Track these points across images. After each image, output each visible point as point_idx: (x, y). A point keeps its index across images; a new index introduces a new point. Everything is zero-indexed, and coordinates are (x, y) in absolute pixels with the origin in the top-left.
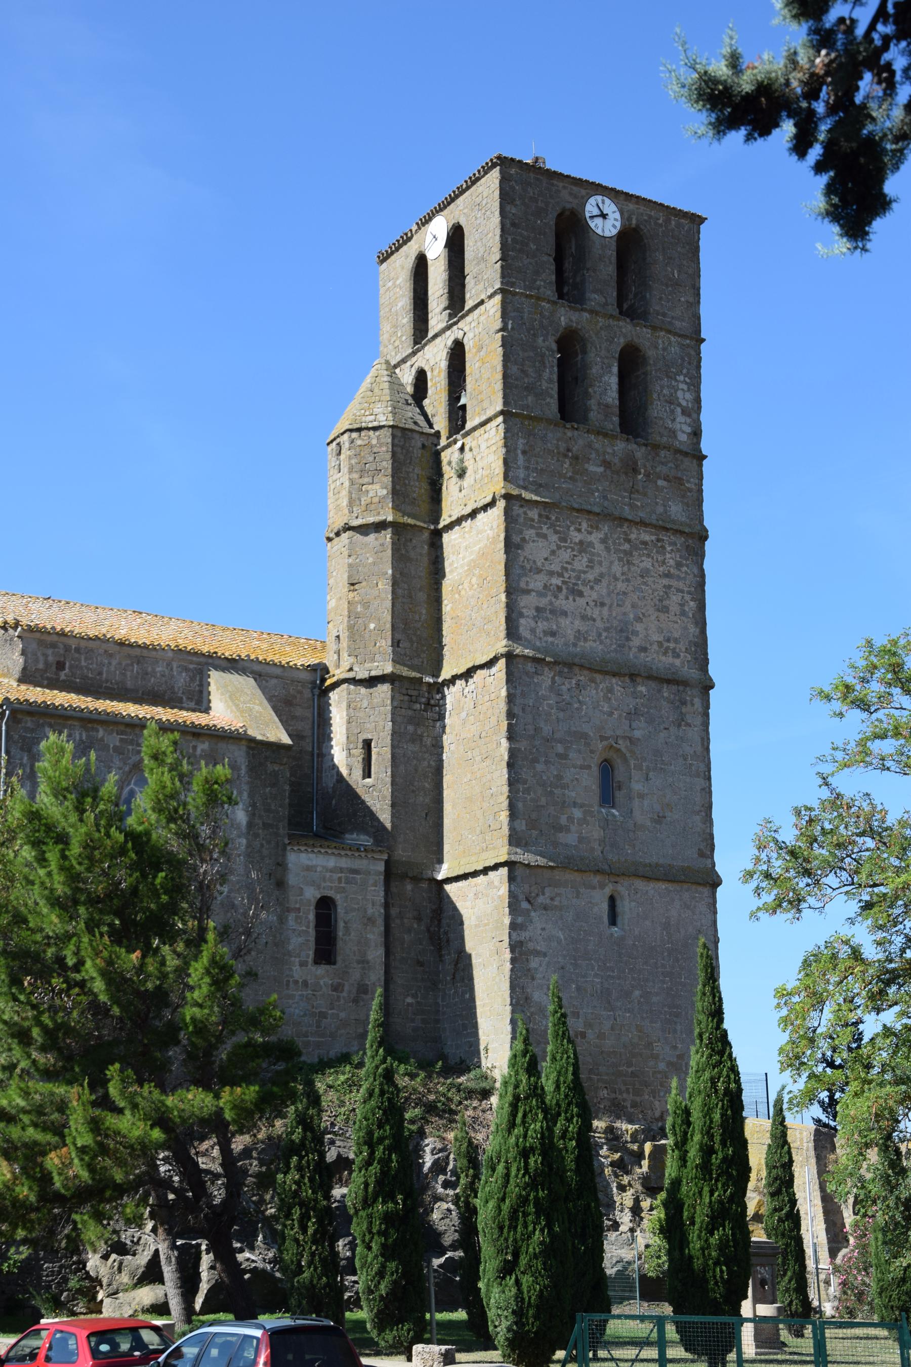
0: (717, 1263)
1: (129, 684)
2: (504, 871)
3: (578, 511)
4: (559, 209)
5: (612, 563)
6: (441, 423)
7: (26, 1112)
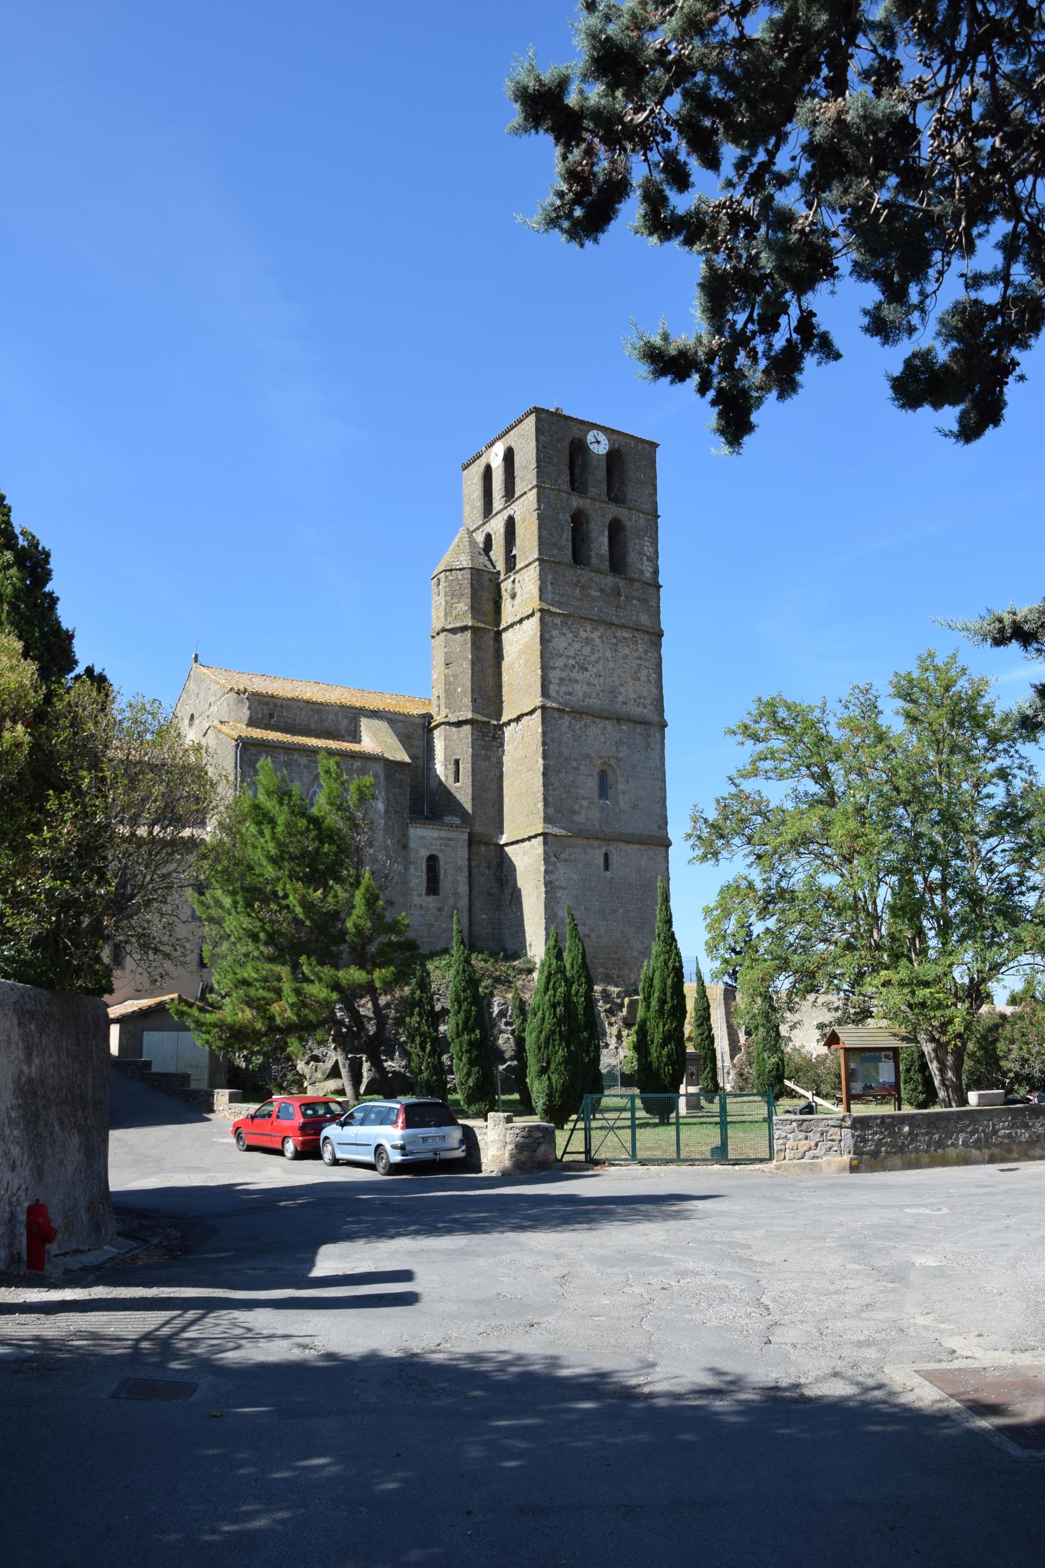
0: (666, 1064)
1: (313, 727)
2: (541, 838)
3: (585, 619)
4: (571, 438)
6: (501, 566)
7: (257, 980)
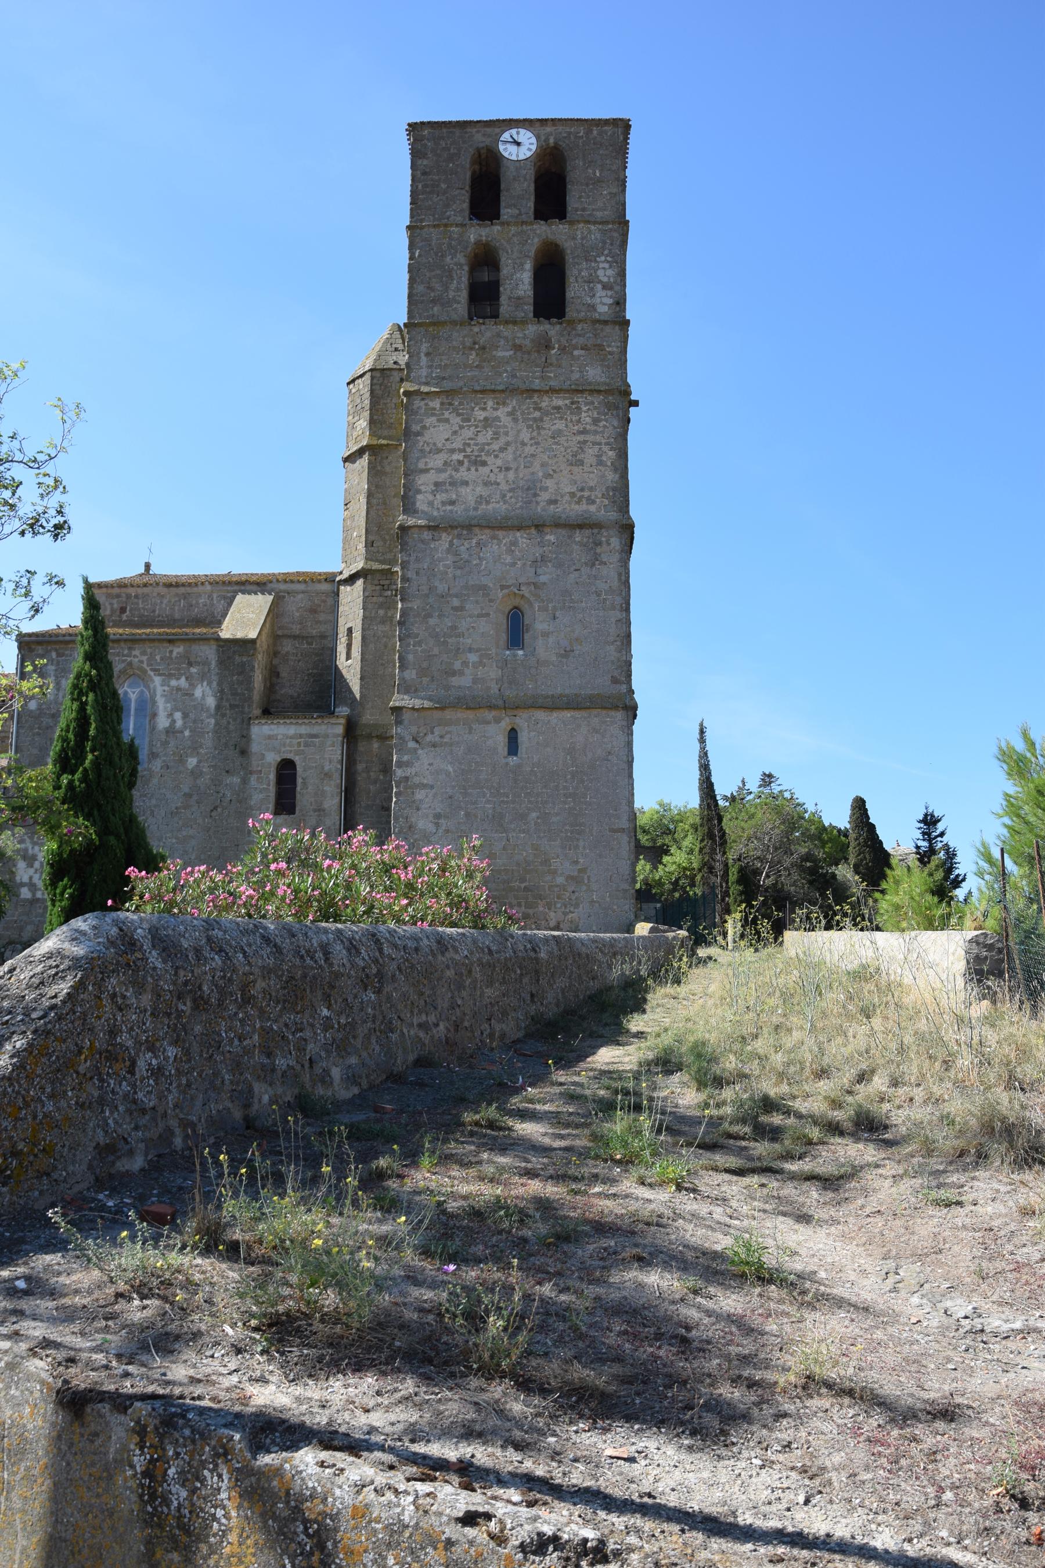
1: (177, 616)
5: (519, 431)
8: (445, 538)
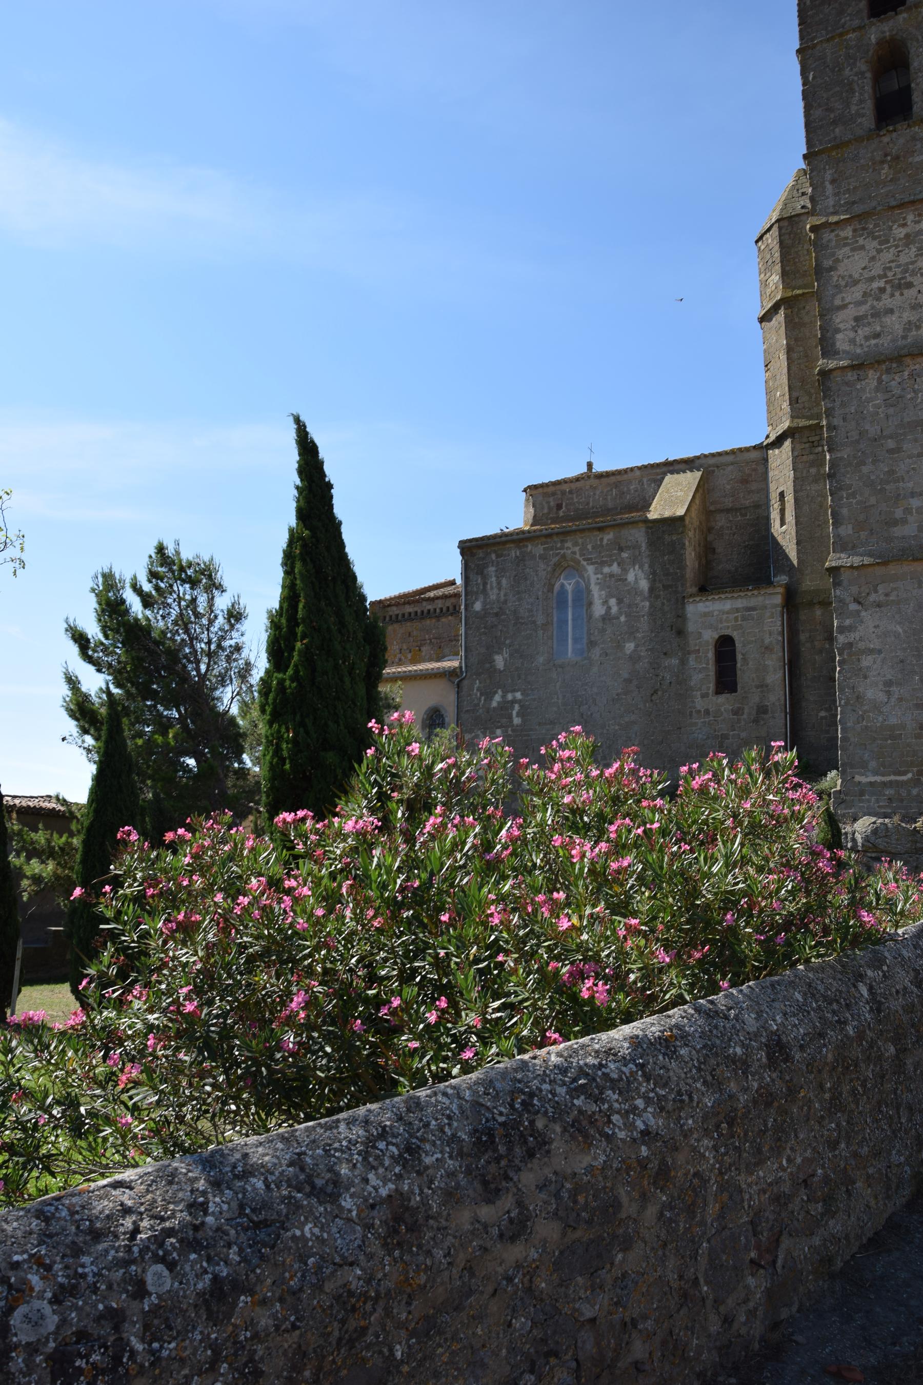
1: (610, 505)
8: (872, 376)
